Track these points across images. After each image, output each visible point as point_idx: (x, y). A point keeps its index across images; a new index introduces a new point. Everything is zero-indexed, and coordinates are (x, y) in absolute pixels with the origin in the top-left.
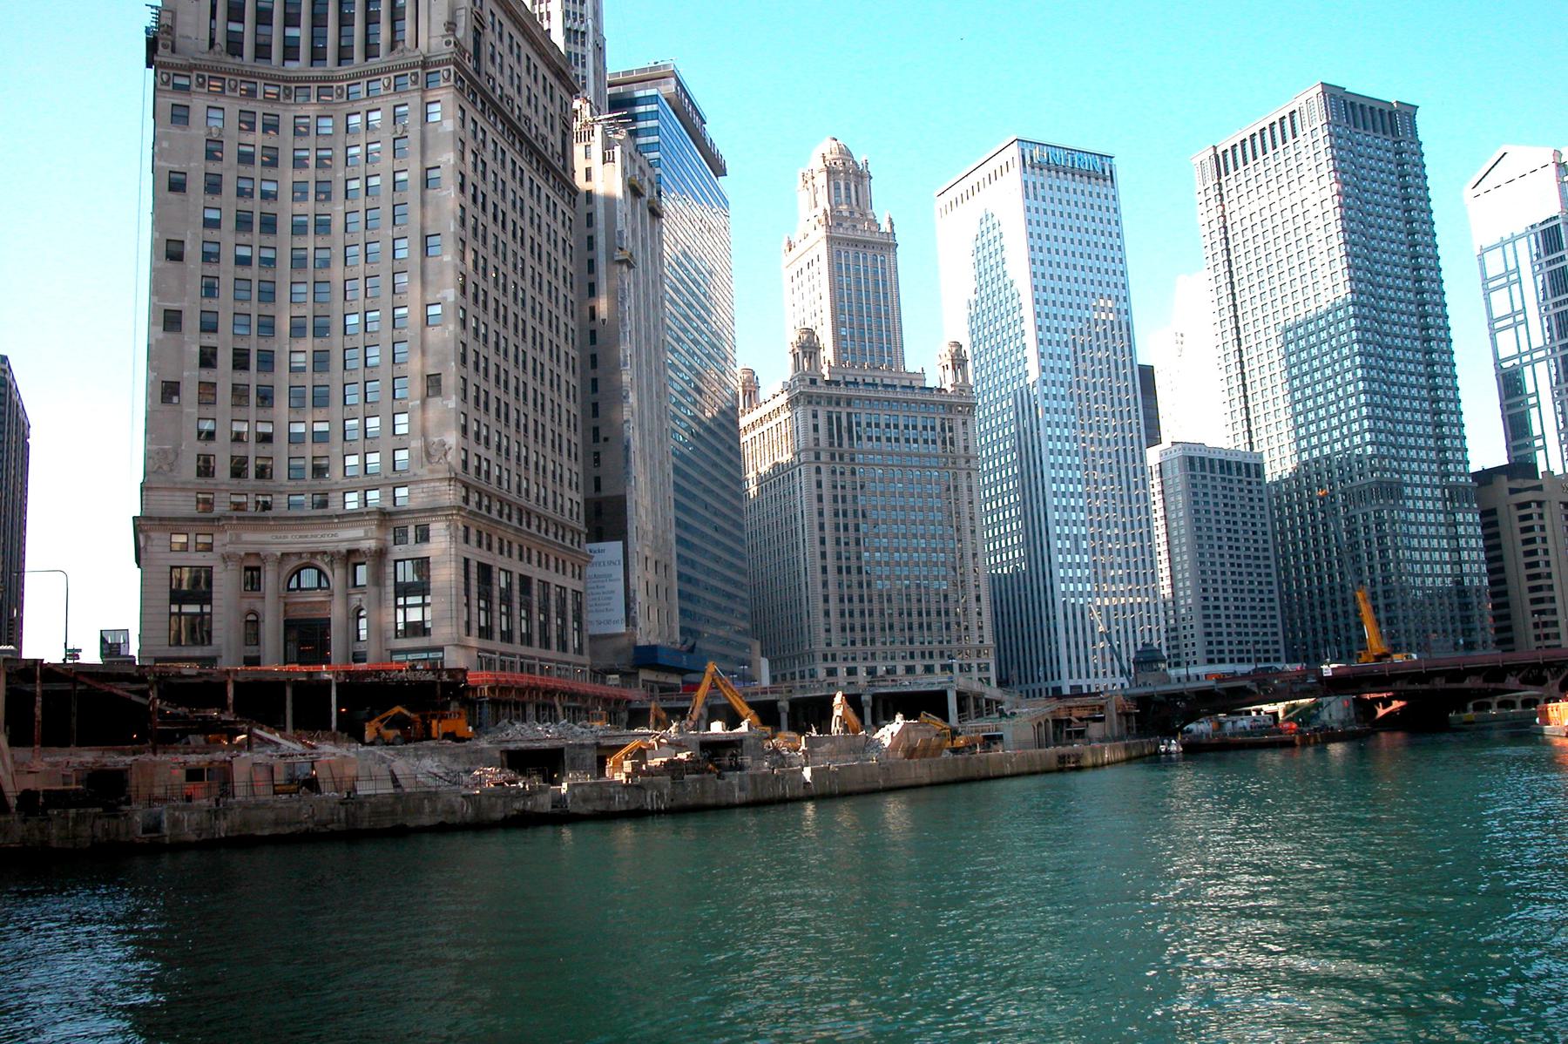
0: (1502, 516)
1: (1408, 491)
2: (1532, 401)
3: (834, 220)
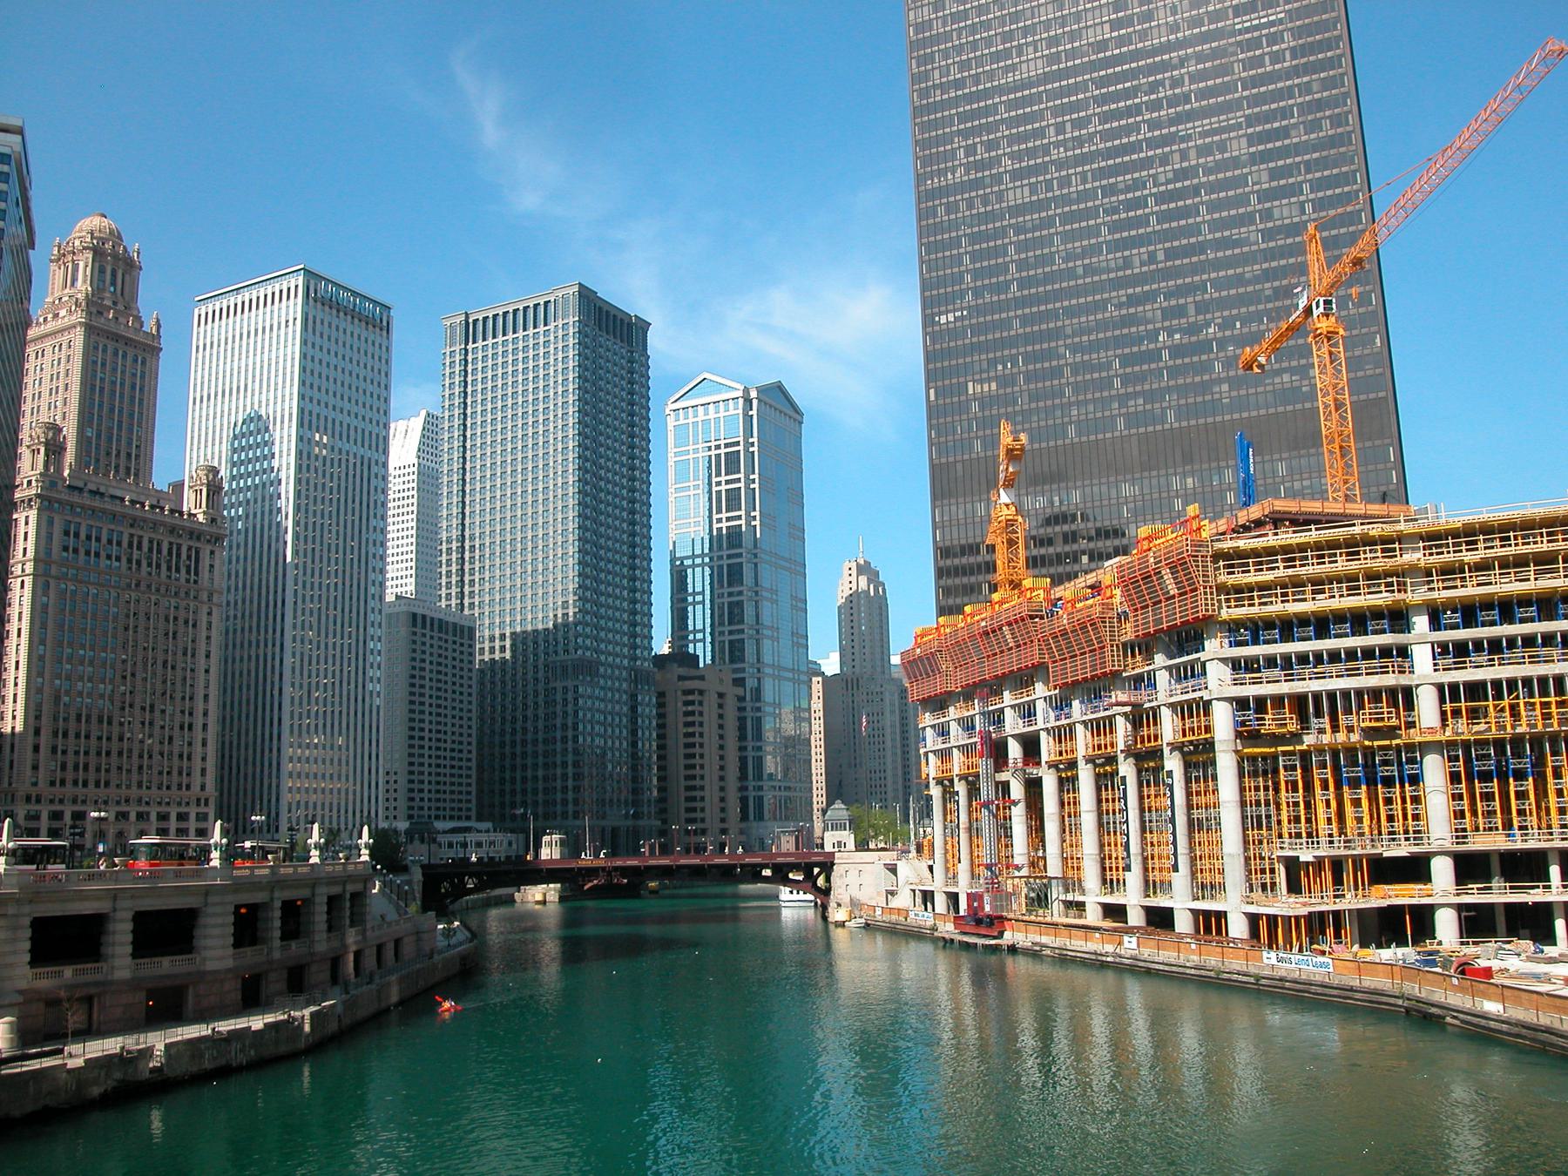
0: (669, 699)
1: (602, 670)
2: (698, 598)
3: (94, 306)
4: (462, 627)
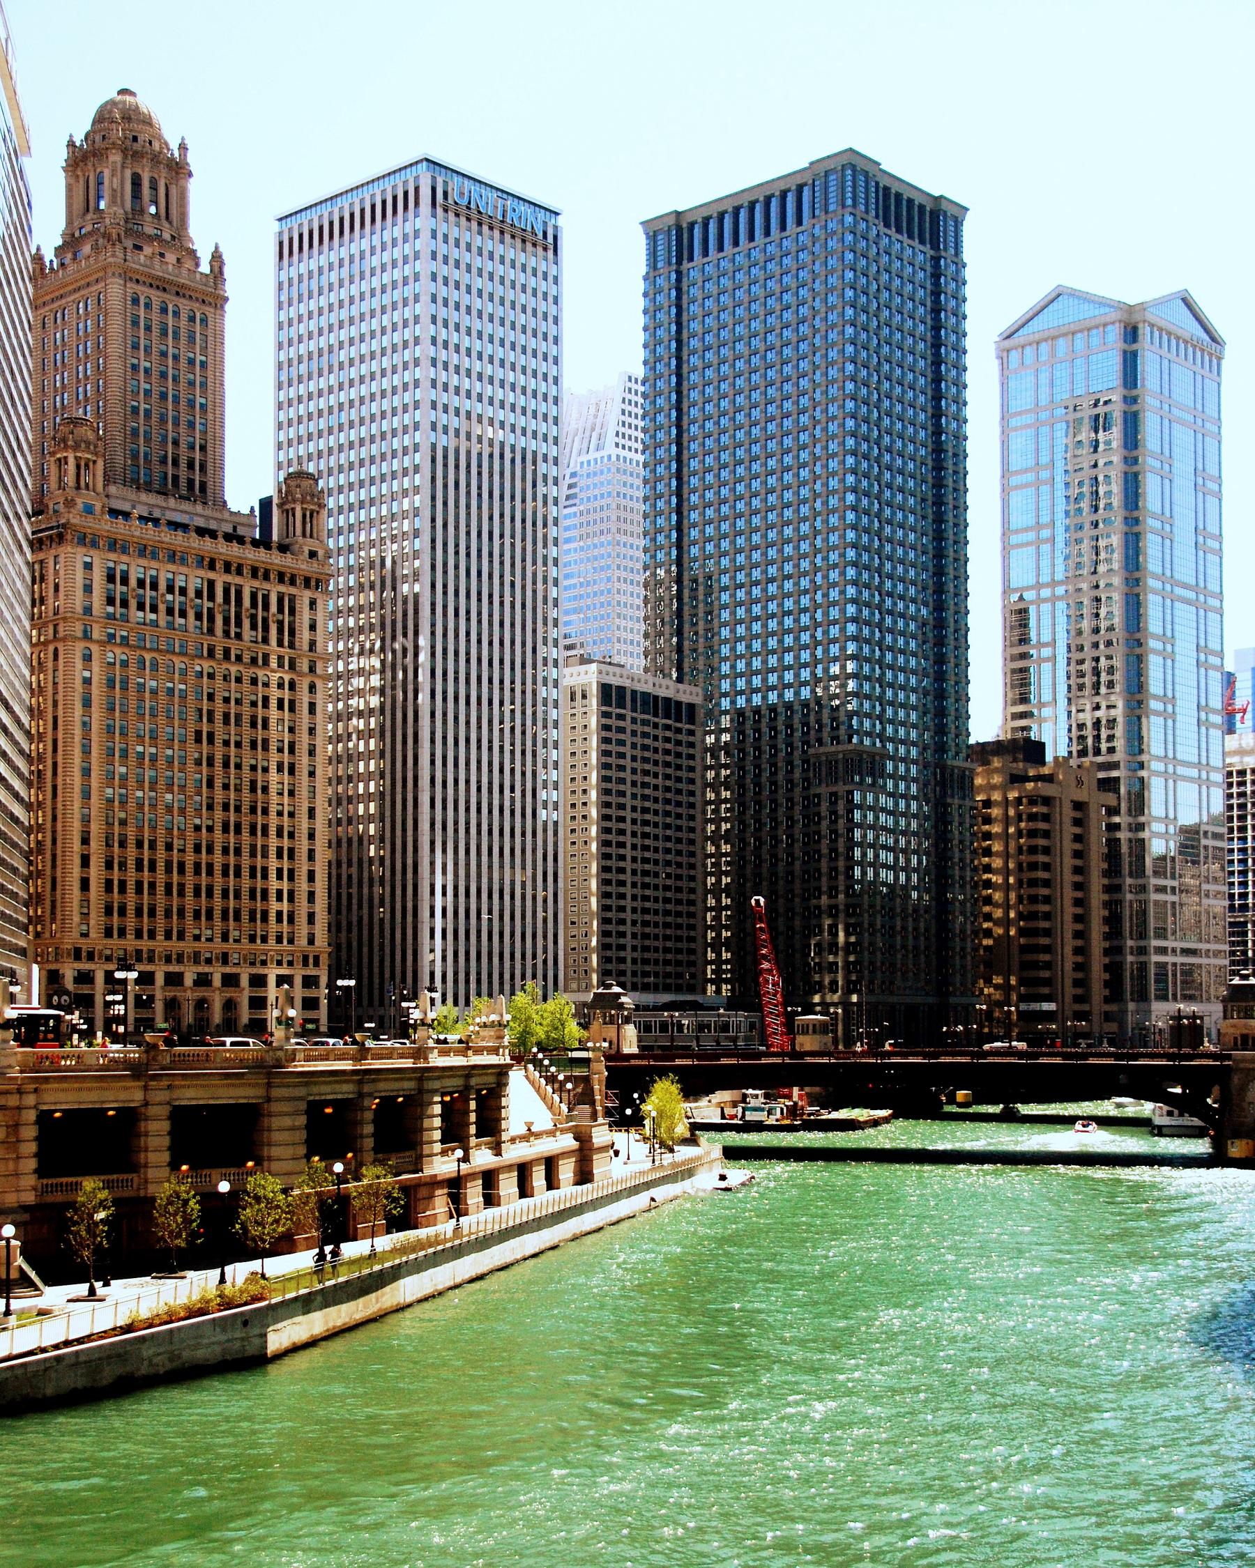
1: (890, 766)
2: (1046, 652)
4: (679, 704)
